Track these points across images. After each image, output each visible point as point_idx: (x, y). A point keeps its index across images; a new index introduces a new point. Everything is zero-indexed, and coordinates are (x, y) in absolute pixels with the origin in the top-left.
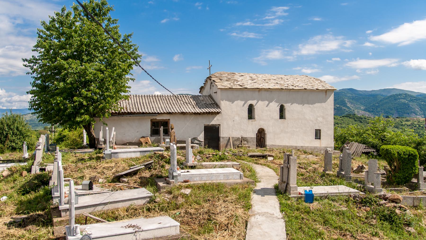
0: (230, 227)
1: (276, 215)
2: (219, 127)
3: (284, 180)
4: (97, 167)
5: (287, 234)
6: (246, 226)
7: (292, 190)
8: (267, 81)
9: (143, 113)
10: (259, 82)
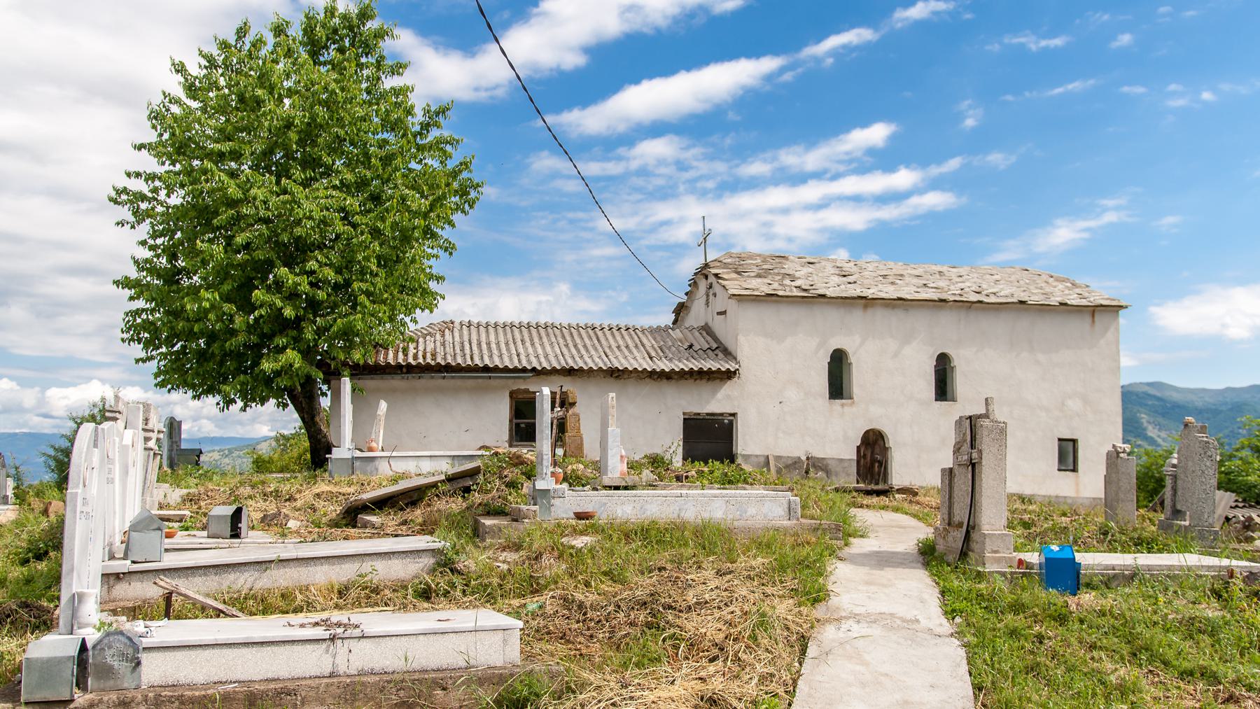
0: (731, 648)
1: (924, 623)
2: (731, 423)
3: (957, 519)
4: (298, 496)
5: (978, 688)
6: (803, 651)
7: (988, 547)
8: (891, 279)
9: (486, 369)
10: (866, 282)
